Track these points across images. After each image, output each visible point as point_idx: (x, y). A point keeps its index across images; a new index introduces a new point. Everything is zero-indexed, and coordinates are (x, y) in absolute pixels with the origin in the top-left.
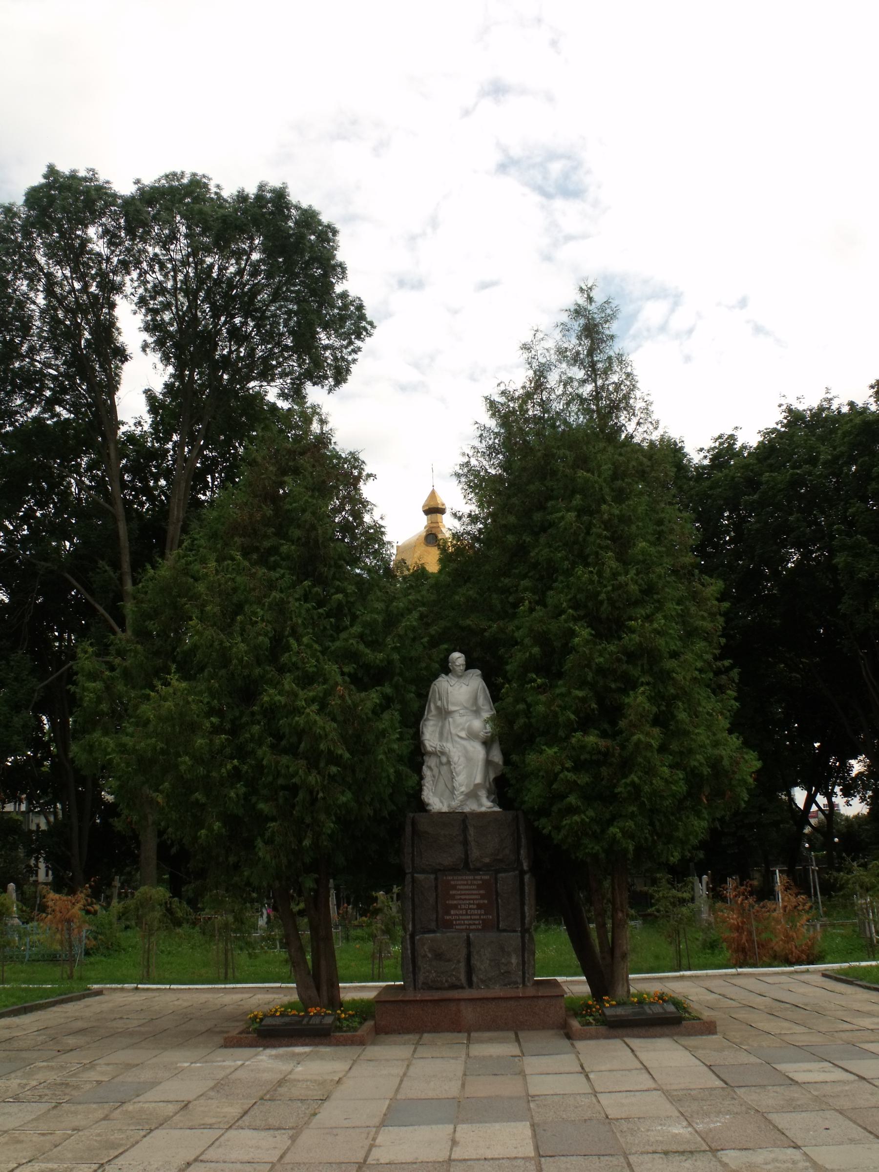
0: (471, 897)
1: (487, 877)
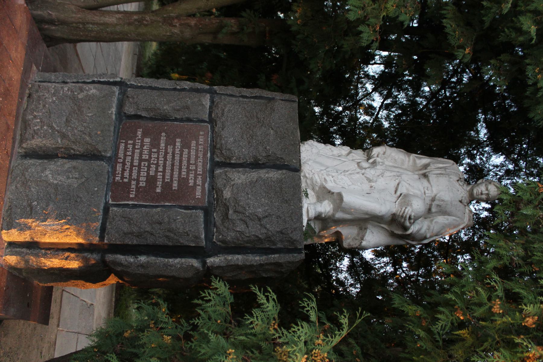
0: (168, 169)
1: (198, 194)
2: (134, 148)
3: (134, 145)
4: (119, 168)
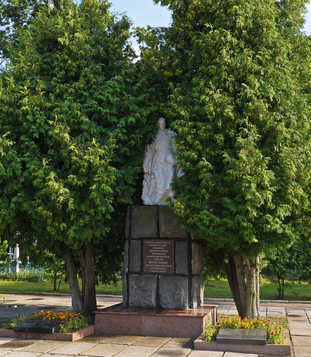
0: (161, 254)
2: (153, 267)
3: (152, 267)
4: (161, 272)
